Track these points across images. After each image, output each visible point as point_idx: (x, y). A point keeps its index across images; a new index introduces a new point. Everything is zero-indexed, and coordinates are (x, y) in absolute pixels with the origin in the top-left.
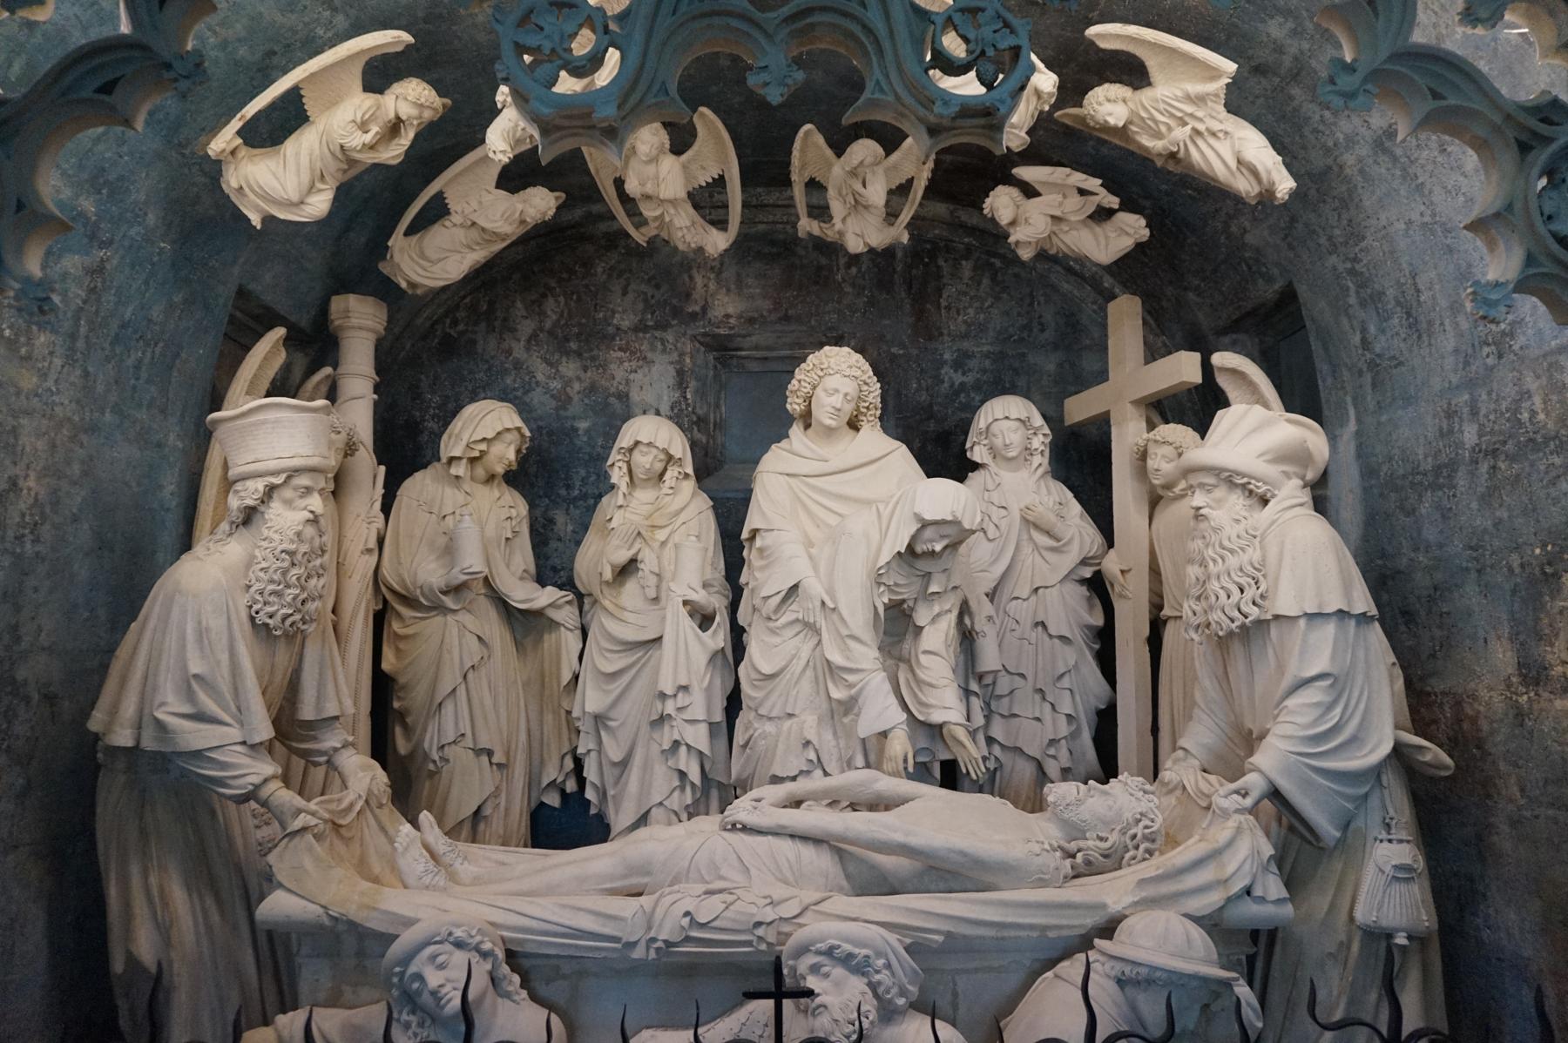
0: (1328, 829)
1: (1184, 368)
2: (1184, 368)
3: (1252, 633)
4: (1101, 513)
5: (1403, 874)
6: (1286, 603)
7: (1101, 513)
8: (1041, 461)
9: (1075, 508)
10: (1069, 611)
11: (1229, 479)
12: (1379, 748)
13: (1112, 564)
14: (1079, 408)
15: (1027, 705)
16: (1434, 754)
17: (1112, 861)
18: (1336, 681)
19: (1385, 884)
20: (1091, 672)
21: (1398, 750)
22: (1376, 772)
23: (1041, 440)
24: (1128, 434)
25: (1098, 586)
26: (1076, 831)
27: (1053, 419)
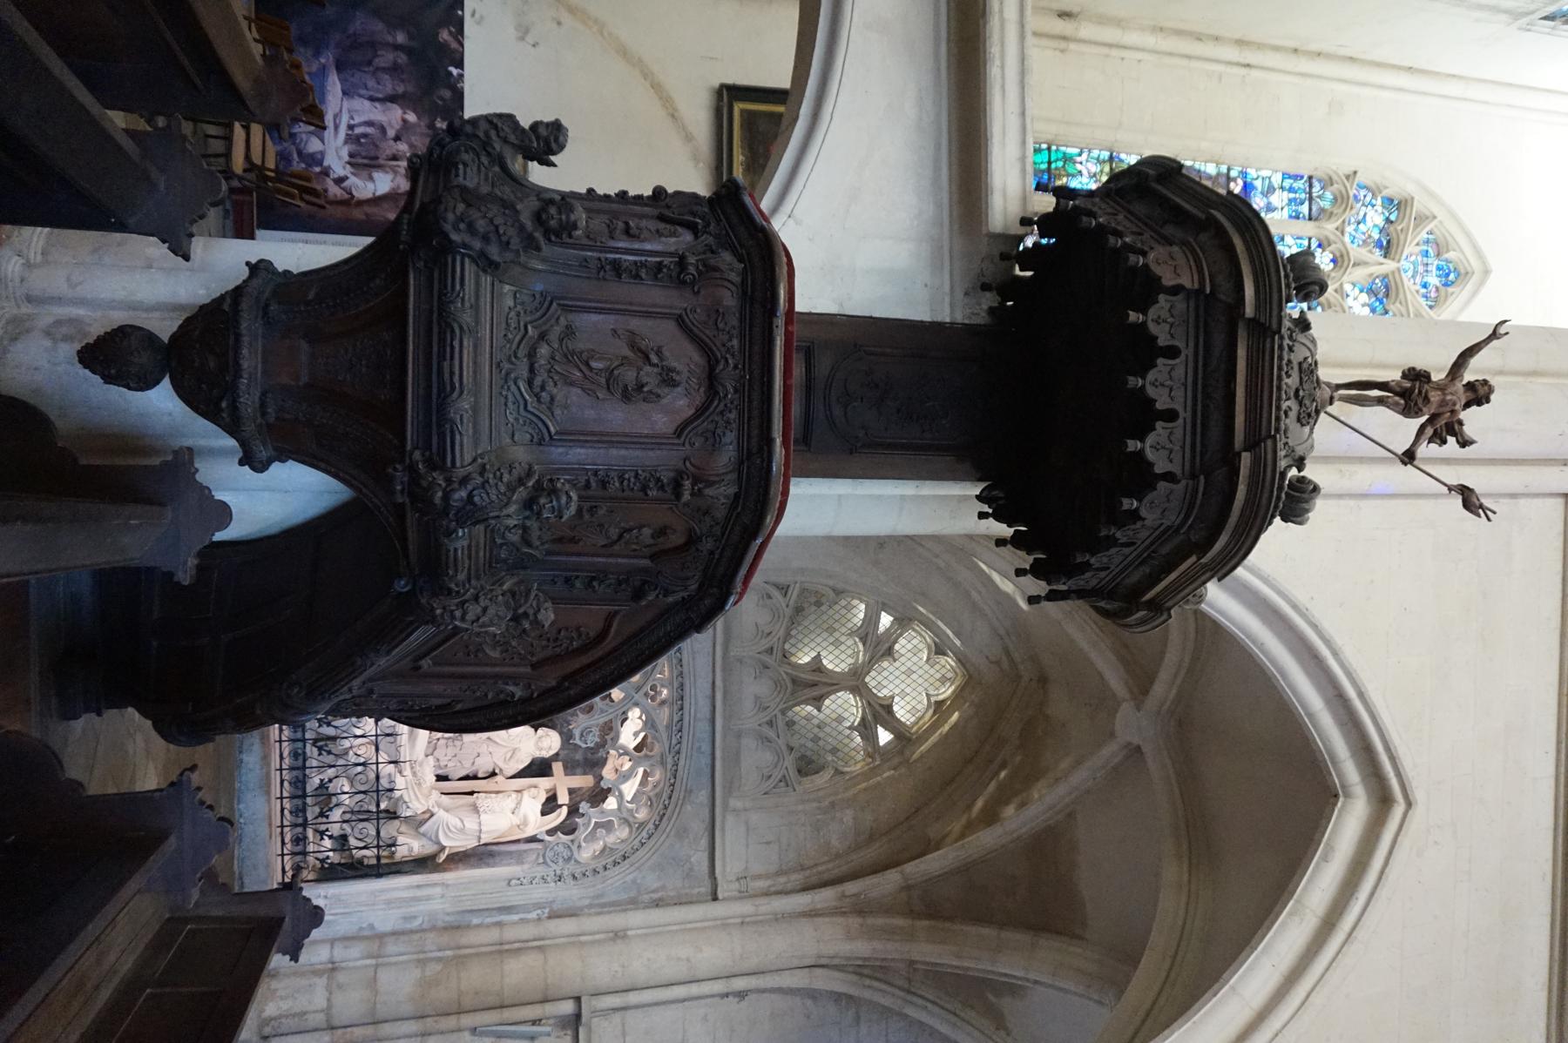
0: (422, 830)
1: (563, 798)
2: (563, 798)
3: (475, 809)
4: (521, 774)
5: (411, 850)
6: (483, 817)
7: (521, 774)
8: (538, 754)
9: (521, 766)
10: (483, 766)
11: (519, 803)
12: (445, 843)
13: (499, 778)
14: (557, 767)
15: (451, 752)
16: (443, 857)
17: (414, 774)
18: (462, 830)
19: (410, 846)
20: (463, 773)
21: (443, 848)
22: (438, 843)
23: (546, 754)
24: (544, 783)
25: (493, 774)
26: (421, 765)
27: (556, 757)
